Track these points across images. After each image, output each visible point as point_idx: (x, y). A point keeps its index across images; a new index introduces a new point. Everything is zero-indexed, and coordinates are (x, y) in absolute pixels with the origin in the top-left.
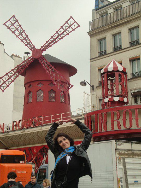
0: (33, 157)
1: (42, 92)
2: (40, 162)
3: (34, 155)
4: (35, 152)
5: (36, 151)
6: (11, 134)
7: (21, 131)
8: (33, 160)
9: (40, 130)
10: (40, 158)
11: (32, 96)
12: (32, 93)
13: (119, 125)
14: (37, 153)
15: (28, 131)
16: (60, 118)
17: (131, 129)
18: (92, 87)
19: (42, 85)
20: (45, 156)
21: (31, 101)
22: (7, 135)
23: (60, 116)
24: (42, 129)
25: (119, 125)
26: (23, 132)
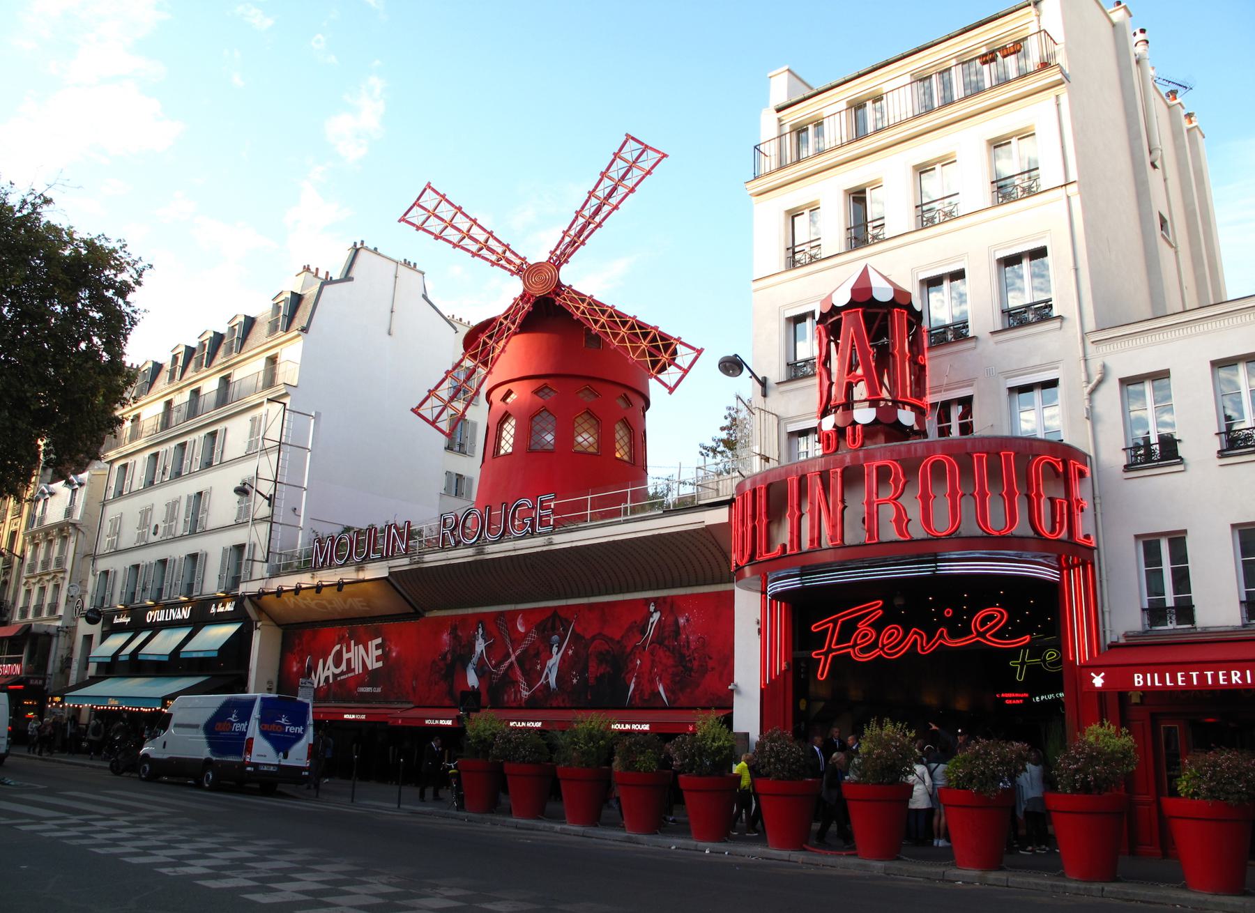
0: (511, 650)
1: (551, 418)
2: (539, 667)
4: (521, 629)
5: (523, 625)
6: (434, 559)
7: (471, 551)
8: (513, 658)
9: (545, 549)
10: (537, 655)
11: (512, 432)
12: (513, 423)
13: (901, 520)
14: (526, 634)
16: (622, 506)
17: (953, 536)
18: (763, 383)
19: (553, 394)
21: (510, 450)
22: (418, 563)
23: (623, 498)
24: (551, 544)
25: (901, 520)
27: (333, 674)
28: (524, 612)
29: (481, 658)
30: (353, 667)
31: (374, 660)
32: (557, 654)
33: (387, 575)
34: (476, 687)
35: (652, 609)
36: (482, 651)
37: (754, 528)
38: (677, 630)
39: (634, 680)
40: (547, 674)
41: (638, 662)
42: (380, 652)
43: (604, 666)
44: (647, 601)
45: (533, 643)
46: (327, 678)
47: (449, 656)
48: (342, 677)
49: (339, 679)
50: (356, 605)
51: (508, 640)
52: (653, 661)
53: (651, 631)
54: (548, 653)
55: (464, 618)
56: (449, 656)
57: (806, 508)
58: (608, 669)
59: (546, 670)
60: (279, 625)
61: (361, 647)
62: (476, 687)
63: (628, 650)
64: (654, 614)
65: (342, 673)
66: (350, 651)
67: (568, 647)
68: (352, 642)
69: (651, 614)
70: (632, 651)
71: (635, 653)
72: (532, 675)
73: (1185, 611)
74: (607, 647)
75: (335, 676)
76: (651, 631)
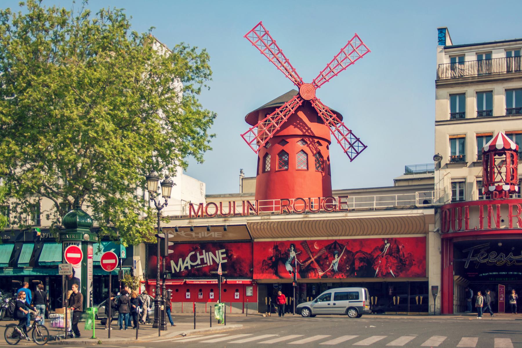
0: (311, 256)
2: (328, 263)
3: (314, 253)
5: (317, 246)
8: (313, 259)
10: (327, 258)
14: (320, 250)
15: (313, 217)
26: (304, 218)
27: (191, 265)
28: (319, 242)
30: (205, 262)
32: (338, 258)
33: (246, 223)
34: (292, 271)
35: (386, 242)
36: (294, 256)
38: (398, 250)
39: (378, 268)
40: (333, 267)
42: (225, 256)
43: (363, 263)
44: (384, 239)
46: (186, 268)
47: (274, 259)
48: (198, 267)
49: (195, 267)
50: (215, 236)
51: (309, 252)
52: (387, 261)
53: (386, 250)
54: (333, 257)
55: (282, 243)
56: (274, 259)
57: (485, 215)
58: (365, 264)
59: (332, 264)
61: (211, 254)
62: (292, 271)
63: (375, 257)
64: (387, 244)
65: (198, 265)
66: (203, 255)
68: (204, 251)
69: (386, 244)
70: (377, 257)
71: (378, 259)
74: (364, 256)
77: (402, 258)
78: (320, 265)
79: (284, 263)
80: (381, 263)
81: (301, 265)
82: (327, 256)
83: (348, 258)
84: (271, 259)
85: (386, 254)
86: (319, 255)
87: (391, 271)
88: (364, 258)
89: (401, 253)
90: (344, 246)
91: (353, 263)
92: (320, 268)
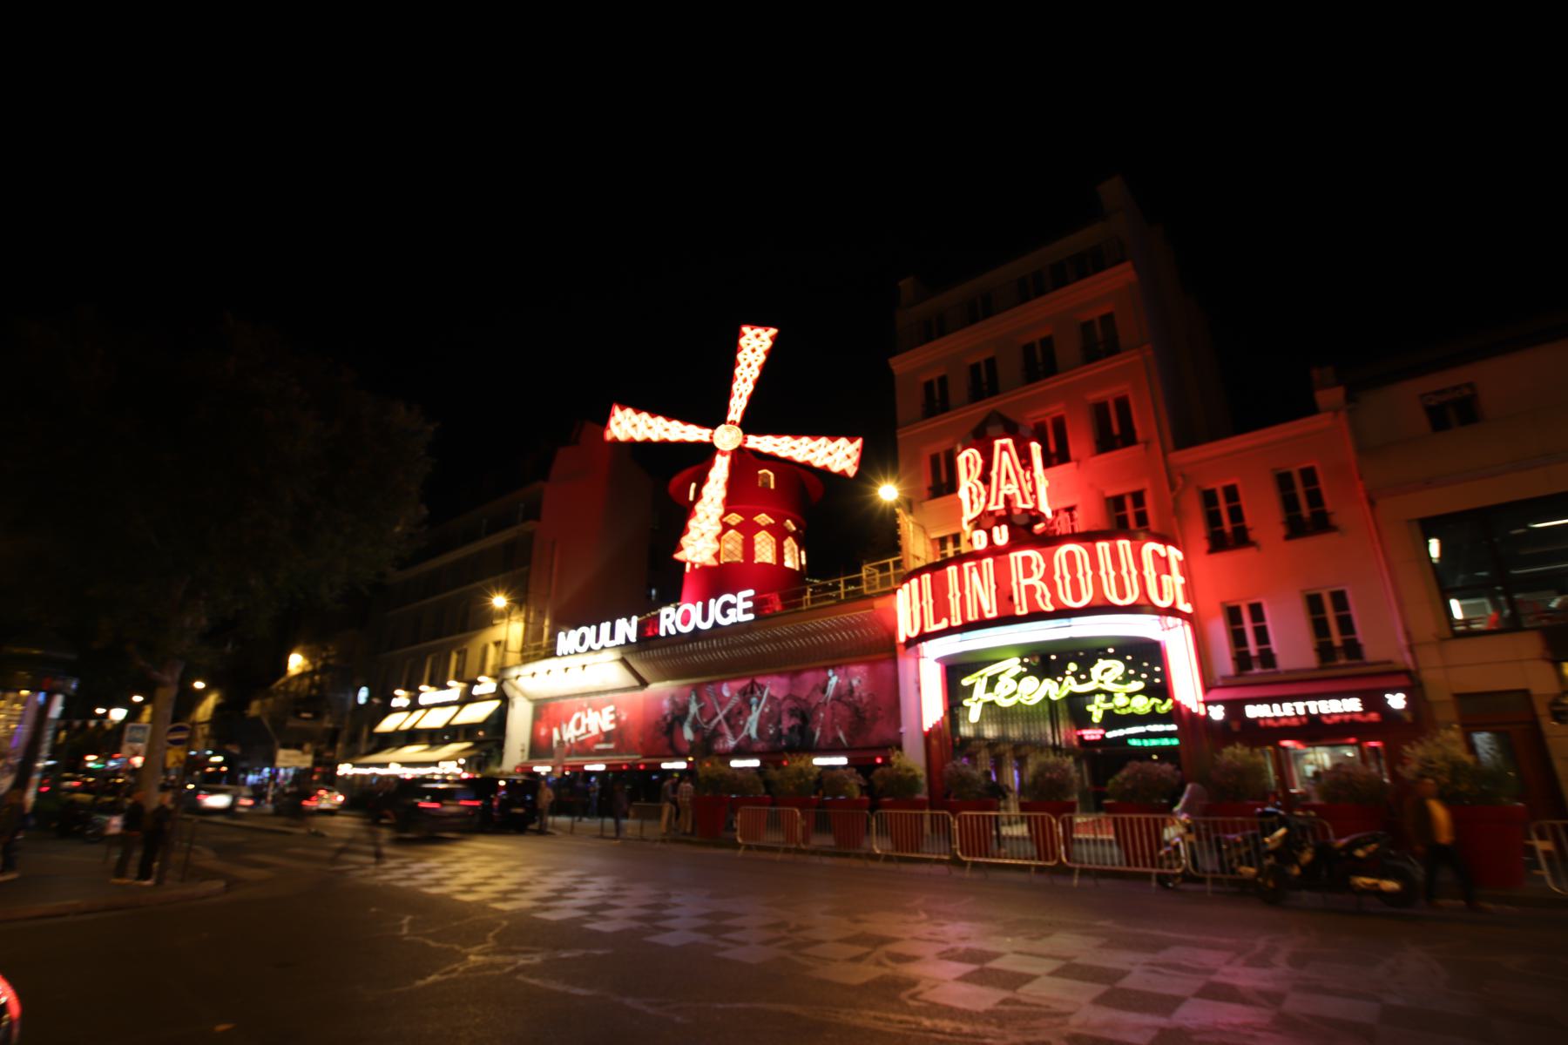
2: (741, 723)
4: (726, 693)
8: (720, 717)
10: (740, 713)
14: (730, 699)
20: (758, 705)
29: (695, 718)
31: (608, 723)
36: (695, 714)
37: (922, 609)
38: (851, 691)
41: (822, 715)
42: (612, 717)
45: (736, 704)
51: (716, 703)
52: (833, 714)
53: (831, 690)
56: (669, 718)
59: (748, 725)
60: (531, 700)
61: (597, 713)
63: (813, 706)
65: (583, 735)
67: (765, 706)
68: (590, 711)
69: (829, 678)
72: (736, 729)
73: (1267, 658)
75: (576, 737)
76: (831, 690)
77: (859, 705)
78: (731, 727)
79: (681, 725)
80: (824, 718)
81: (704, 729)
82: (740, 709)
83: (771, 710)
84: (665, 718)
85: (832, 699)
86: (730, 705)
87: (841, 735)
88: (797, 708)
89: (857, 694)
90: (765, 688)
91: (779, 722)
92: (732, 733)
